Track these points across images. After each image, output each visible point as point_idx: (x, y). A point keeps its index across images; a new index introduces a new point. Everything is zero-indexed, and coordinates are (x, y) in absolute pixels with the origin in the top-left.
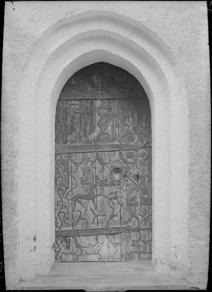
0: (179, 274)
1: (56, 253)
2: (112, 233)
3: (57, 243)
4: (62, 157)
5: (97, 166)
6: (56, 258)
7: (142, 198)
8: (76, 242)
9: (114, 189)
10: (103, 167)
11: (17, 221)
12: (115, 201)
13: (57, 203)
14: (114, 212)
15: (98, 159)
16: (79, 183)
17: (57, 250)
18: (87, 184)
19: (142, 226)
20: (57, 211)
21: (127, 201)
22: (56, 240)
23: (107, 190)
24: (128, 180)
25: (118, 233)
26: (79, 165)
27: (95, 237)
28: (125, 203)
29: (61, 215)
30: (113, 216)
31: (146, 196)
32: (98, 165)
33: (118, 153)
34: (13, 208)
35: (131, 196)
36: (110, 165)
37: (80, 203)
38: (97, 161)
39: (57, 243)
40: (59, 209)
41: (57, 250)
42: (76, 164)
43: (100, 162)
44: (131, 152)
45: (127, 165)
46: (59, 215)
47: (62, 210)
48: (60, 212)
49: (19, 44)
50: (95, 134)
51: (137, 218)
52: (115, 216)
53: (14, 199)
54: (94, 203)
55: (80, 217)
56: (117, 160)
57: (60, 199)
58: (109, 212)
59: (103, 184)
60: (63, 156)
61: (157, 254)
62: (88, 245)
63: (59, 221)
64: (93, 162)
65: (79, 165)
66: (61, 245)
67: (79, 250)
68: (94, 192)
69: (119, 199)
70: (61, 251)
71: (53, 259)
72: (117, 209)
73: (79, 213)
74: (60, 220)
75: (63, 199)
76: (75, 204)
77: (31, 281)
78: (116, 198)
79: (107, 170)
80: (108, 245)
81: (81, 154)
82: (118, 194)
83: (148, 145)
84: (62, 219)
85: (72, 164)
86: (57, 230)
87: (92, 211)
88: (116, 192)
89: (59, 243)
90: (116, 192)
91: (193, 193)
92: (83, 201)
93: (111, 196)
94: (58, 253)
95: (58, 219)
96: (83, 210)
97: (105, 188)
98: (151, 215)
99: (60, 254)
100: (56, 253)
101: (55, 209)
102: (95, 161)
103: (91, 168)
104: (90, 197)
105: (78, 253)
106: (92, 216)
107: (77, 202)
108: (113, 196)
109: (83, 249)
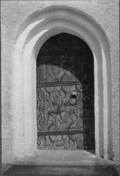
1: (38, 145)
2: (71, 133)
3: (39, 139)
4: (41, 89)
5: (62, 94)
8: (50, 139)
9: (72, 107)
10: (65, 94)
11: (13, 125)
12: (73, 115)
13: (38, 116)
15: (62, 89)
16: (51, 105)
17: (39, 143)
18: (56, 105)
20: (39, 121)
21: (80, 115)
22: (38, 138)
23: (68, 108)
24: (81, 102)
26: (51, 94)
27: (61, 136)
29: (41, 123)
30: (72, 123)
32: (62, 93)
33: (74, 86)
34: (10, 118)
36: (70, 93)
38: (62, 91)
39: (39, 139)
40: (39, 119)
41: (39, 143)
42: (49, 93)
43: (63, 91)
45: (80, 93)
46: (39, 123)
47: (41, 120)
48: (40, 122)
49: (12, 26)
50: (61, 75)
52: (74, 123)
53: (10, 113)
54: (60, 116)
55: (52, 124)
57: (40, 114)
58: (70, 121)
59: (65, 105)
60: (41, 88)
63: (40, 127)
64: (59, 92)
65: (51, 94)
66: (41, 140)
68: (60, 110)
69: (75, 113)
70: (41, 144)
72: (75, 119)
73: (51, 122)
74: (41, 126)
75: (42, 113)
76: (49, 116)
78: (74, 113)
80: (69, 140)
81: (52, 87)
84: (42, 125)
85: (47, 93)
86: (39, 131)
87: (59, 121)
88: (74, 110)
89: (40, 139)
90: (74, 110)
91: (115, 109)
92: (53, 115)
94: (39, 145)
95: (39, 125)
96: (54, 120)
99: (40, 146)
100: (38, 145)
101: (37, 120)
102: (60, 91)
103: (59, 95)
104: (58, 112)
106: (59, 123)
107: (50, 116)
109: (53, 142)
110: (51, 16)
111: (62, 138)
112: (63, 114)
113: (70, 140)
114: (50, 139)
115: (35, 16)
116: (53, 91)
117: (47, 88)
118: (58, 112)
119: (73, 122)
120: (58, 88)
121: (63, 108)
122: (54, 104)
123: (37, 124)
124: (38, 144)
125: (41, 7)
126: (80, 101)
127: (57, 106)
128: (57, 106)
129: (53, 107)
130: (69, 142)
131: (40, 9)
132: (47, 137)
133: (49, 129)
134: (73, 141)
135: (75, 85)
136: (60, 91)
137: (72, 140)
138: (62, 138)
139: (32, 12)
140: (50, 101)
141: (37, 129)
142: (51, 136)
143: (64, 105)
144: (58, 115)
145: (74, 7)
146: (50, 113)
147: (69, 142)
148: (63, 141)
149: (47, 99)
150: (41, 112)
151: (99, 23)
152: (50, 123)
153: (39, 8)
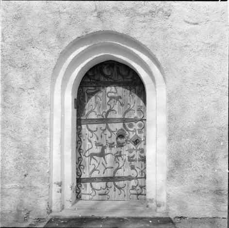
0: (163, 209)
3: (78, 187)
4: (81, 127)
6: (77, 197)
7: (140, 156)
8: (91, 186)
9: (119, 149)
10: (111, 134)
14: (119, 166)
19: (139, 176)
22: (77, 185)
23: (114, 150)
25: (122, 181)
28: (127, 158)
31: (142, 155)
35: (131, 155)
37: (94, 159)
39: (78, 187)
41: (78, 191)
44: (131, 124)
45: (129, 133)
46: (79, 168)
51: (136, 170)
52: (120, 168)
55: (94, 170)
56: (122, 129)
59: (111, 146)
61: (148, 196)
62: (100, 188)
63: (79, 171)
67: (94, 192)
71: (75, 198)
75: (83, 156)
76: (91, 159)
77: (58, 212)
79: (114, 136)
80: (115, 188)
82: (122, 153)
83: (144, 118)
86: (78, 177)
87: (103, 164)
90: (121, 152)
93: (117, 154)
94: (79, 193)
96: (97, 164)
97: (113, 149)
98: (146, 168)
101: (77, 163)
102: (105, 129)
104: (102, 155)
105: (92, 194)
108: (119, 154)
110: (88, 46)
111: (106, 185)
112: (108, 157)
113: (116, 188)
114: (91, 186)
115: (79, 41)
116: (97, 129)
117: (90, 126)
118: (102, 155)
119: (120, 167)
120: (103, 126)
121: (107, 151)
122: (97, 145)
123: (77, 169)
124: (76, 192)
125: (86, 32)
126: (128, 142)
127: (101, 147)
128: (101, 147)
129: (97, 148)
130: (115, 191)
131: (85, 34)
132: (88, 184)
133: (91, 173)
134: (120, 188)
135: (122, 123)
136: (105, 129)
137: (118, 188)
138: (107, 186)
139: (74, 38)
140: (92, 141)
141: (76, 175)
142: (92, 183)
143: (109, 147)
144: (102, 158)
145: (125, 33)
146: (92, 155)
147: (115, 191)
148: (107, 189)
149: (89, 138)
150: (81, 154)
151: (154, 53)
152: (92, 168)
153: (83, 33)
